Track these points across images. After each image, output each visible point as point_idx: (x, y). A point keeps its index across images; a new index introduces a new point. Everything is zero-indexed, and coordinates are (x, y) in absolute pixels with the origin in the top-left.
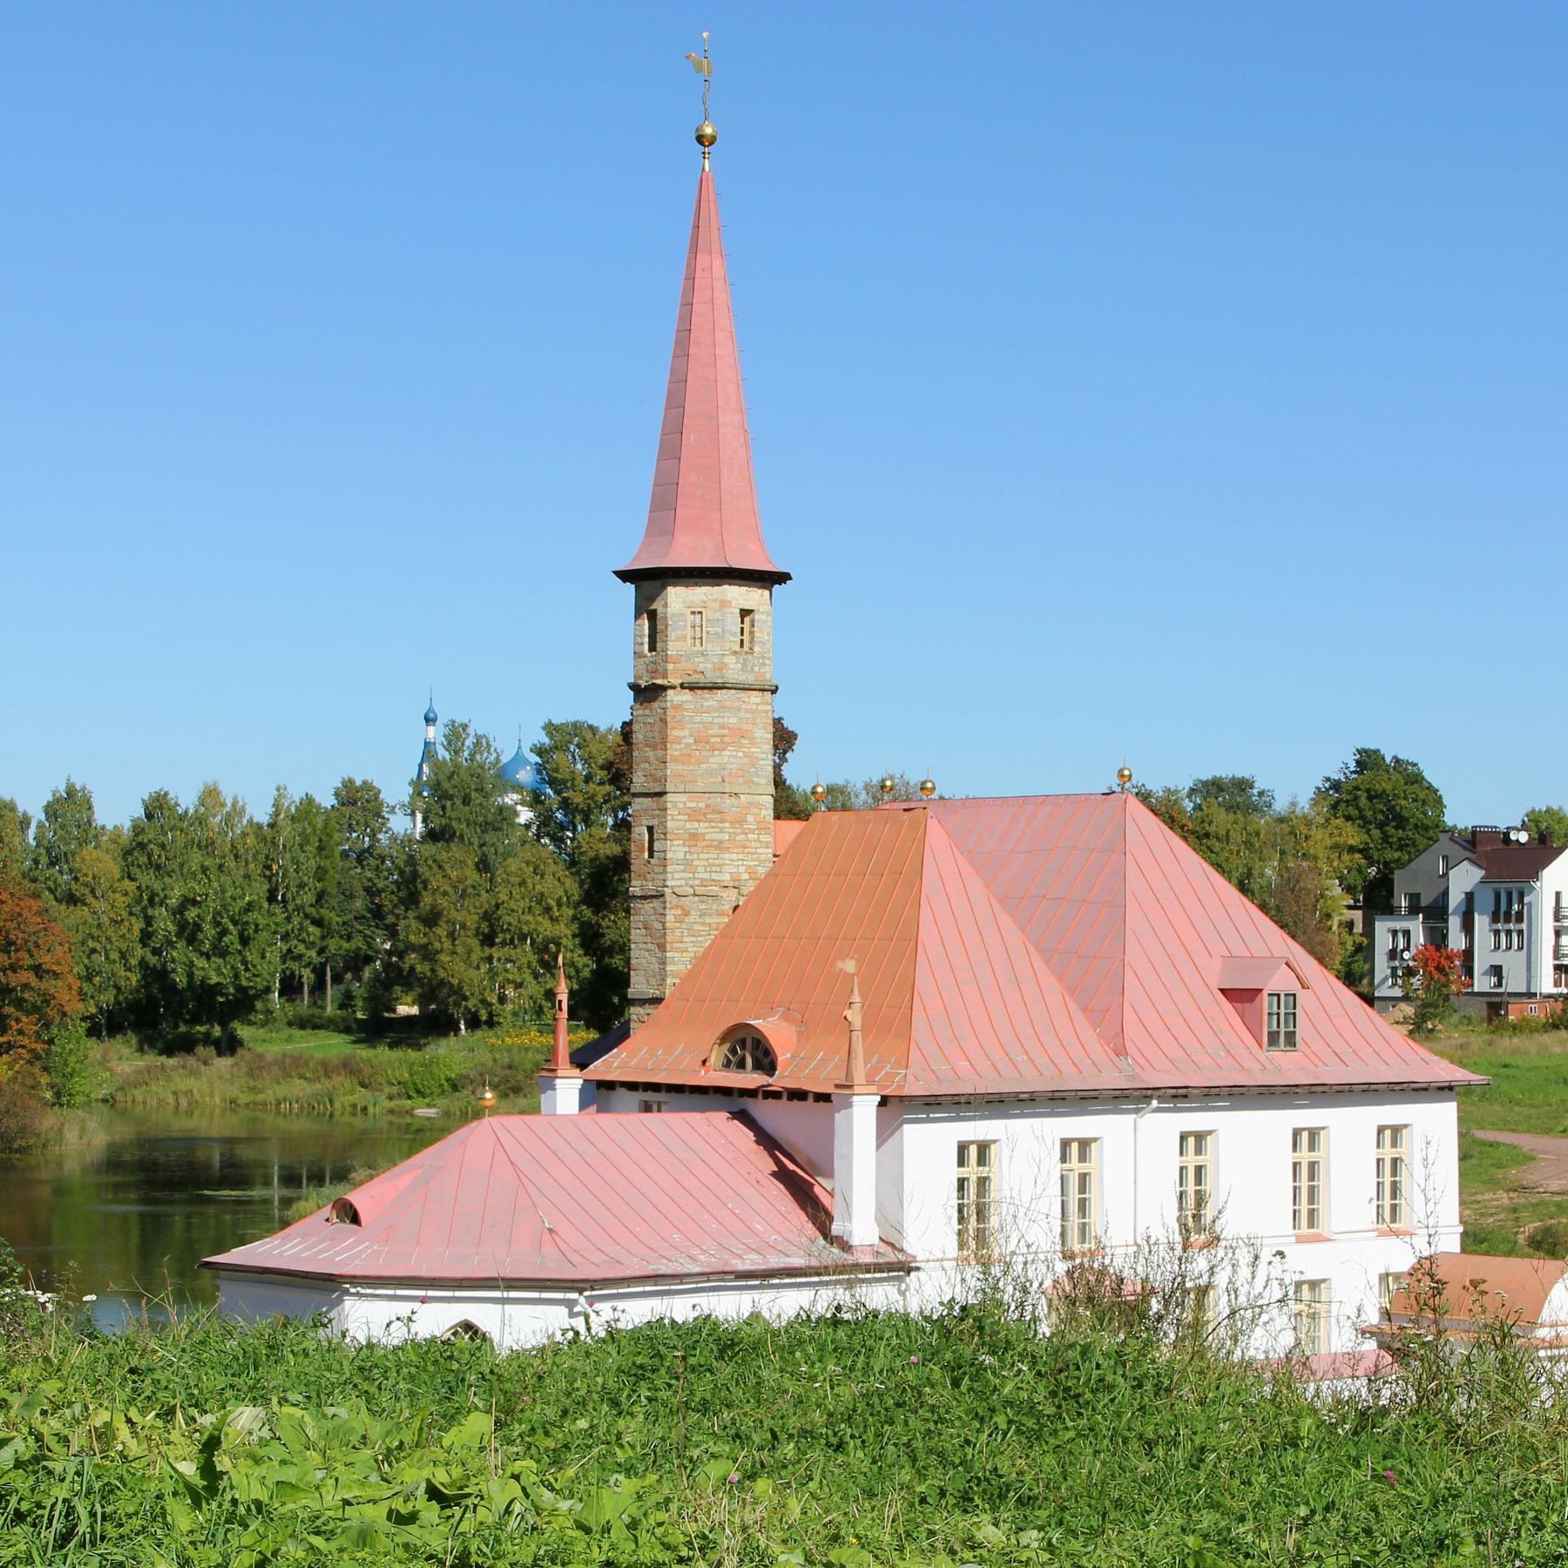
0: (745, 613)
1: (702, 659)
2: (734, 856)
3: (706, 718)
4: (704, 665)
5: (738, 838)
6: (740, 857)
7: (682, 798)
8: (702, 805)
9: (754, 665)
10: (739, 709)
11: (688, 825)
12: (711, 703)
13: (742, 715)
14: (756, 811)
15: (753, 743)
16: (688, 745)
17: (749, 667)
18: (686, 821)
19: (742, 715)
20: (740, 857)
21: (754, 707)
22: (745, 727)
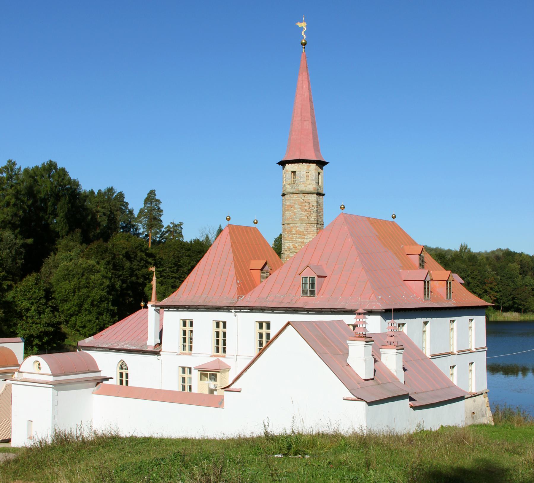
0: (294, 172)
2: (288, 241)
5: (290, 236)
6: (290, 241)
9: (295, 187)
10: (290, 200)
13: (291, 201)
14: (295, 228)
15: (295, 209)
17: (294, 188)
19: (291, 201)
20: (290, 241)
21: (295, 199)
22: (292, 204)
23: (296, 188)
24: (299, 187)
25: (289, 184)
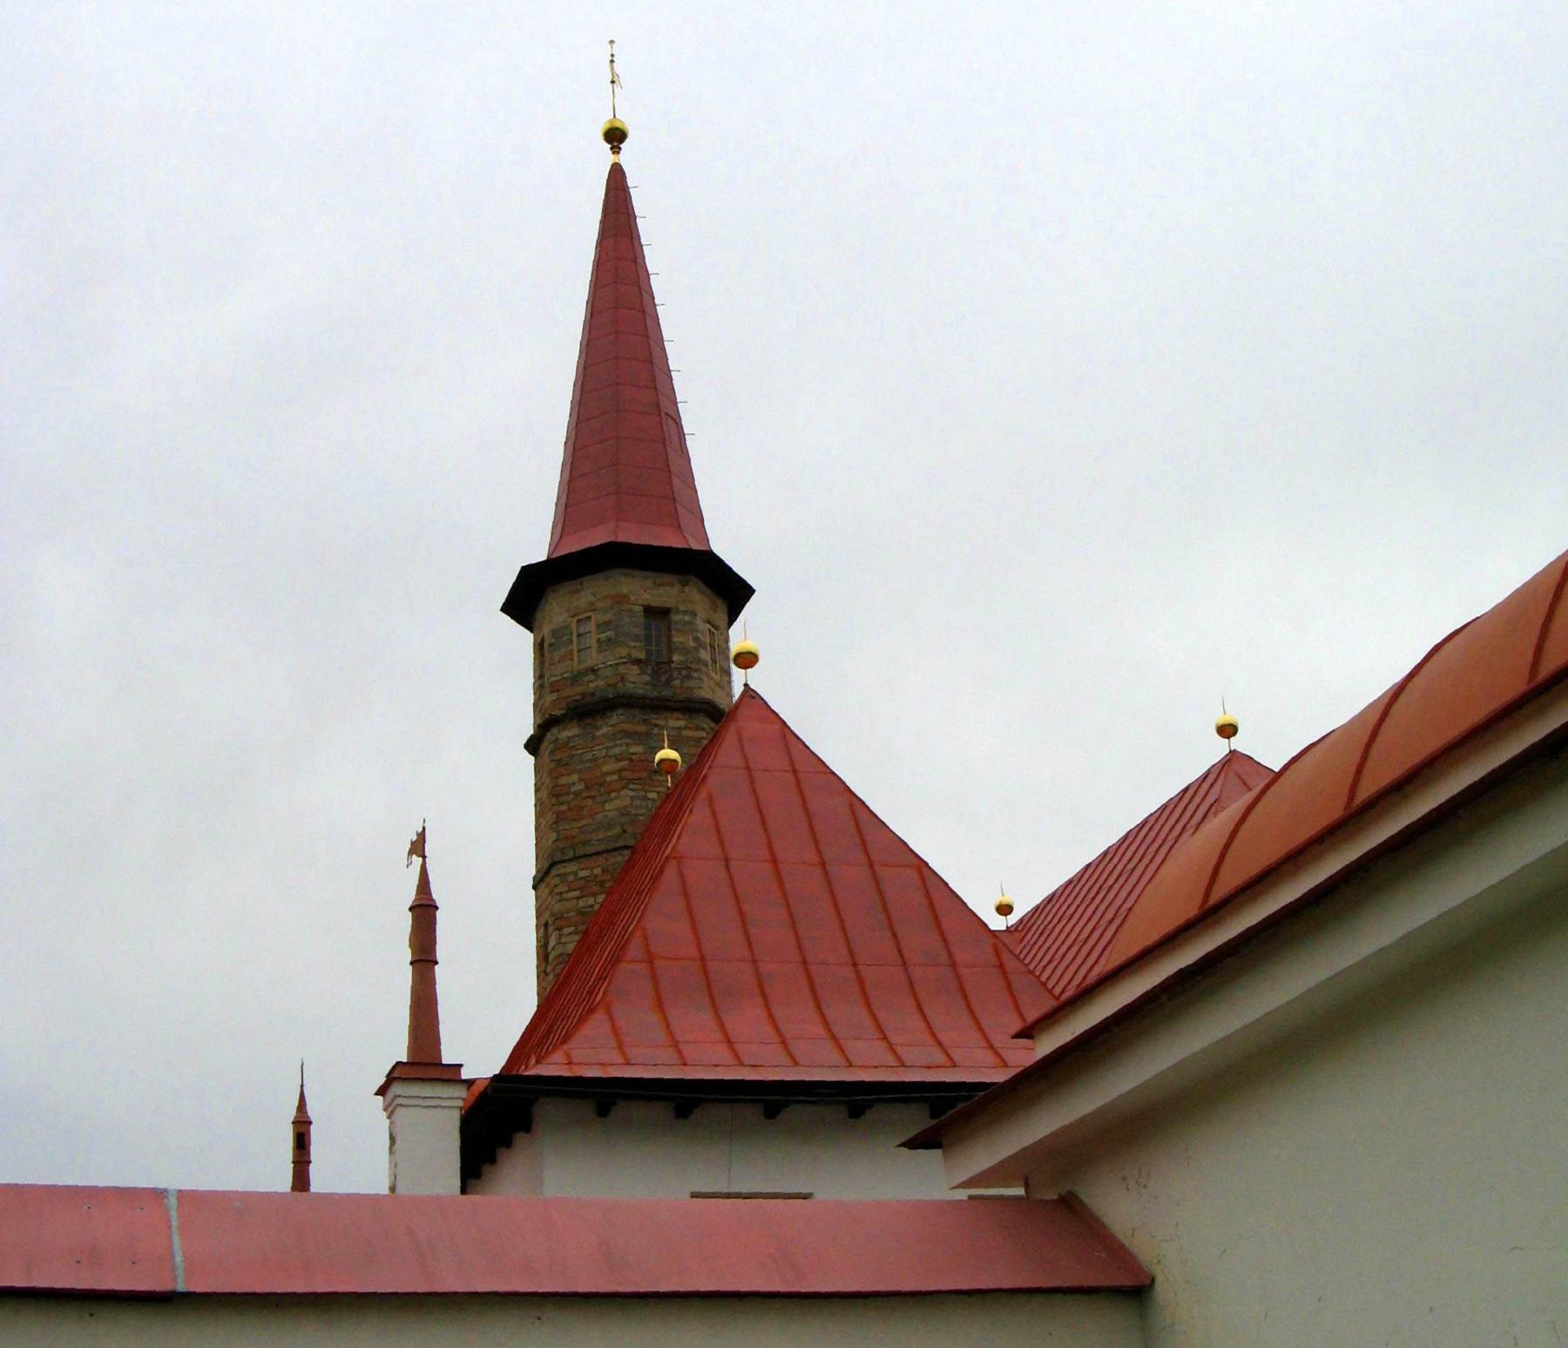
1: (592, 677)
3: (599, 752)
4: (595, 684)
7: (572, 867)
8: (597, 871)
11: (581, 903)
12: (605, 730)
16: (577, 794)
18: (578, 898)
23: (677, 683)
24: (691, 684)
25: (638, 662)
